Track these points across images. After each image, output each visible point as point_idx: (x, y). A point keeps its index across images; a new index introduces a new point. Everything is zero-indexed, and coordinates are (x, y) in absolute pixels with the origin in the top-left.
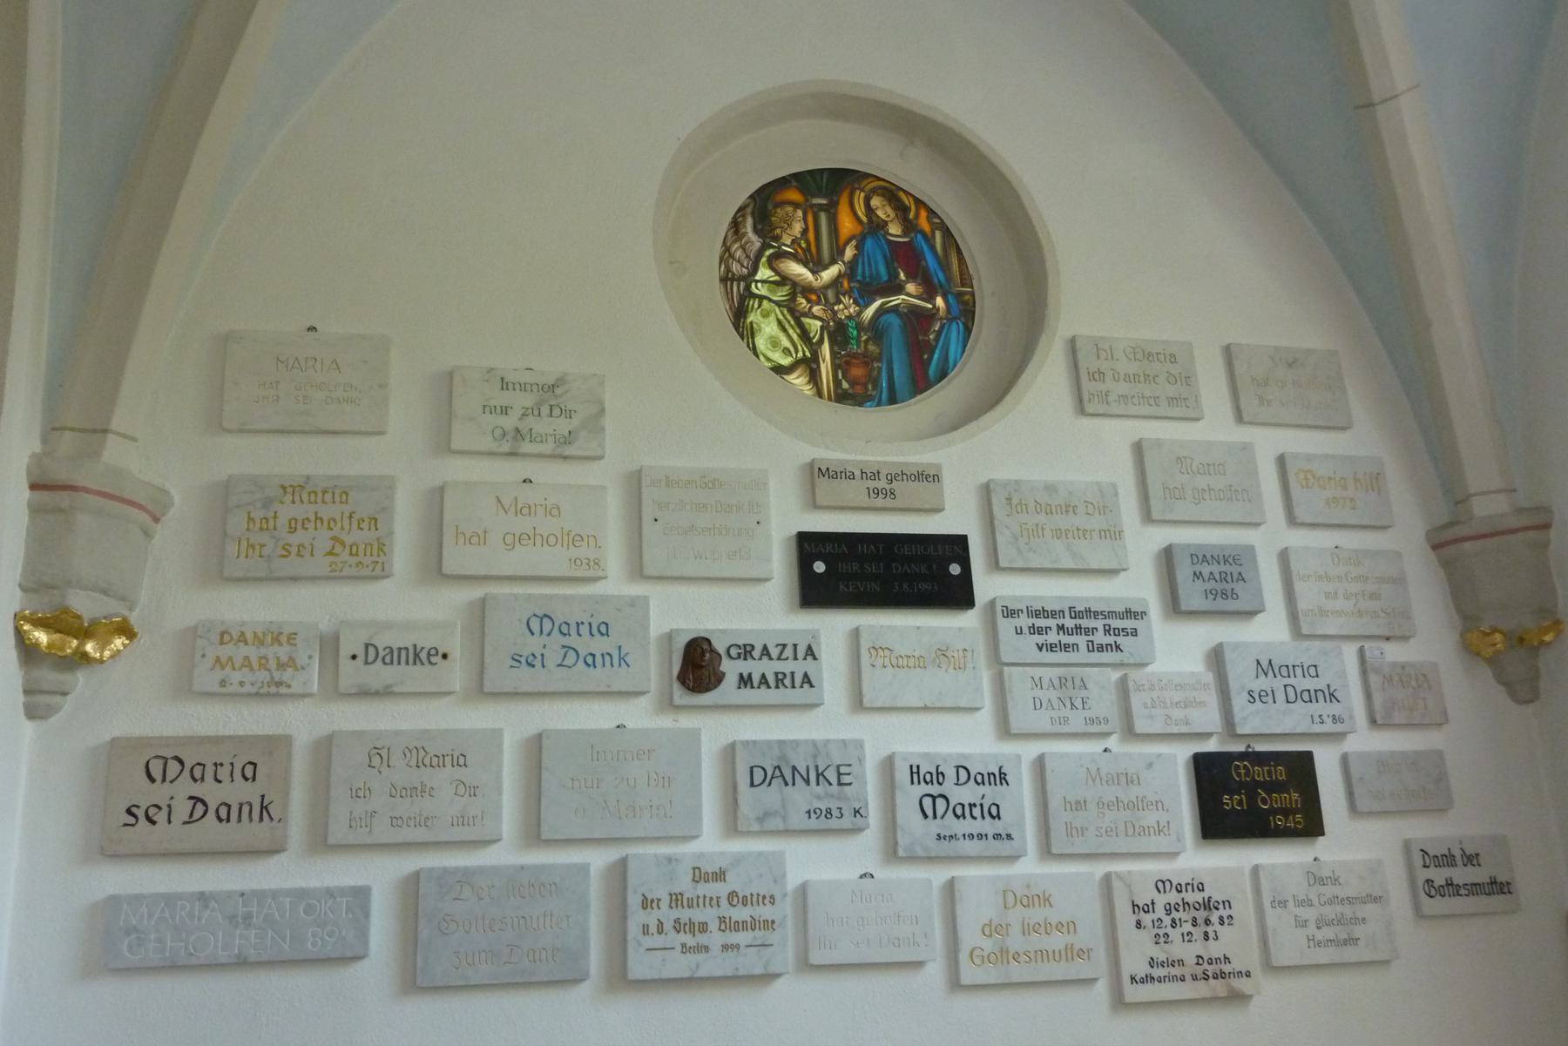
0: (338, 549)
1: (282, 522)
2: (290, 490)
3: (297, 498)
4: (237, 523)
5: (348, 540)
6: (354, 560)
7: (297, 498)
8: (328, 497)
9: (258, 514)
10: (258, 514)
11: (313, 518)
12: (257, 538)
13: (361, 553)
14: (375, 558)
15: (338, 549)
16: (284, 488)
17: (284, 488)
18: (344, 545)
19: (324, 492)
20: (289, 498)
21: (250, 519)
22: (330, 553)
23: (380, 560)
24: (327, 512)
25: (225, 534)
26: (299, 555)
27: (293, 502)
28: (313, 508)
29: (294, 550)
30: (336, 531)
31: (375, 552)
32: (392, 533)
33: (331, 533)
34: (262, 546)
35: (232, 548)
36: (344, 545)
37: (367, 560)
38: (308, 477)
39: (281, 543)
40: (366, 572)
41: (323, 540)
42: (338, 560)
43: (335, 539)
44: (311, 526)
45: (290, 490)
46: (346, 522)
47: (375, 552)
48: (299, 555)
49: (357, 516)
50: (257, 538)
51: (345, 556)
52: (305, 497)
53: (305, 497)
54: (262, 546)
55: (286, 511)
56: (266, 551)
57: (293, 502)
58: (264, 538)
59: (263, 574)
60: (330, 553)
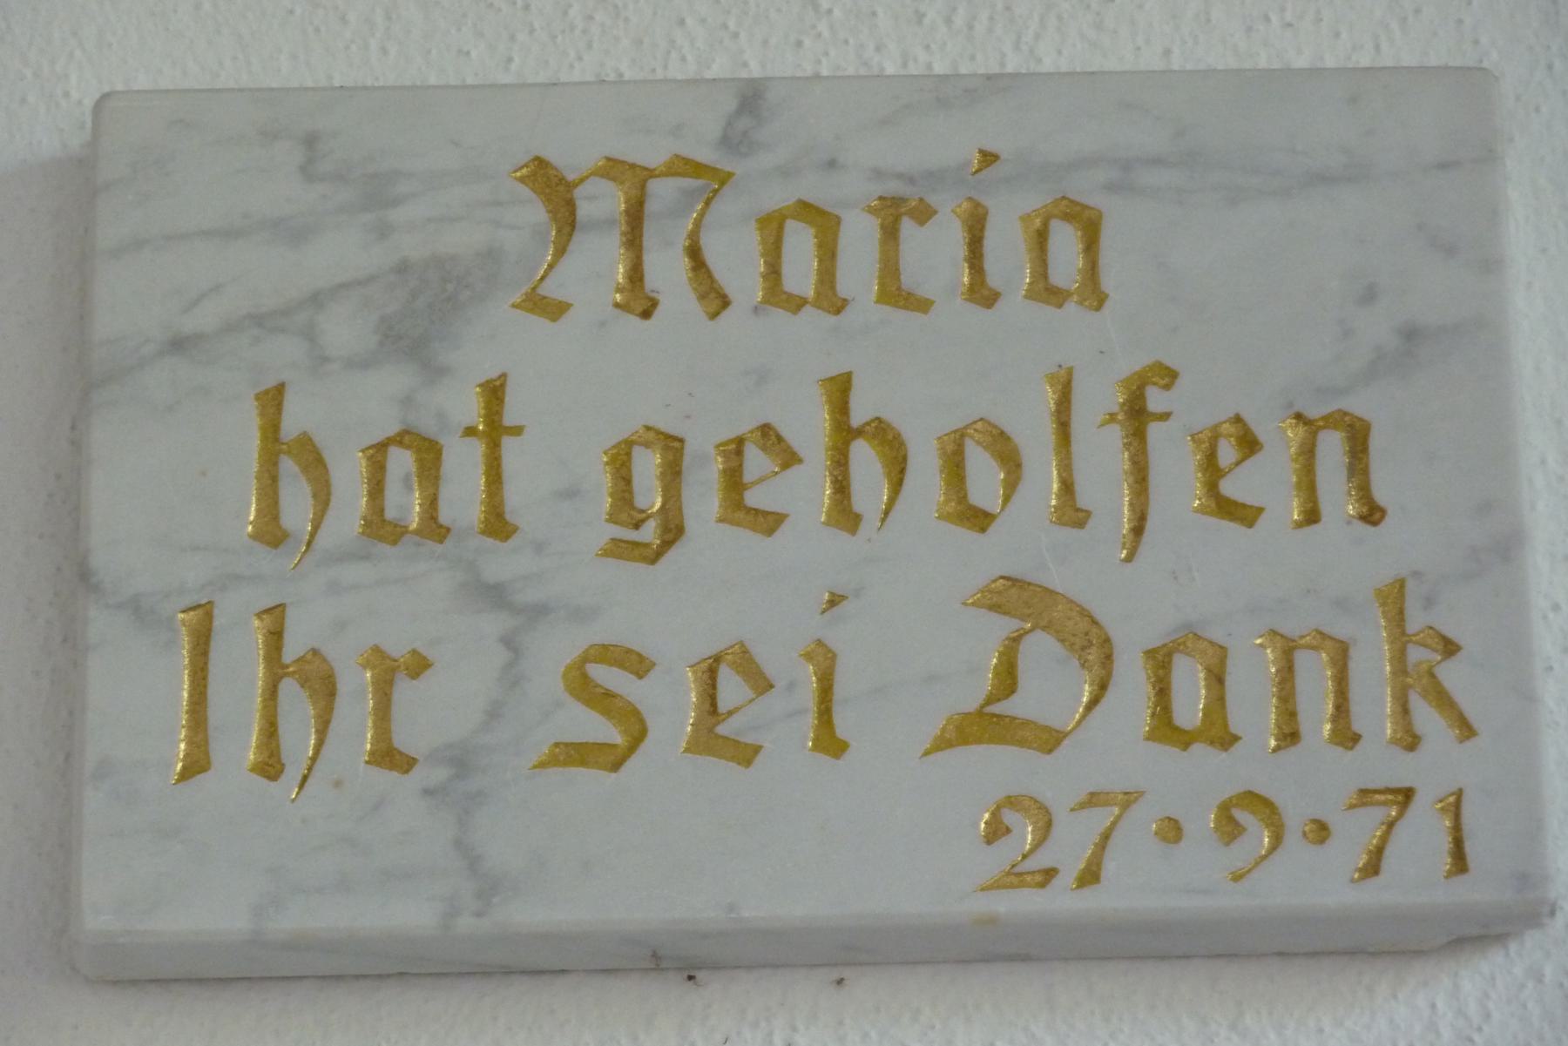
0: (1051, 685)
1: (555, 467)
2: (602, 202)
3: (666, 269)
4: (173, 490)
5: (1137, 611)
6: (1204, 777)
7: (666, 269)
8: (934, 253)
9: (348, 411)
10: (348, 411)
11: (809, 428)
12: (348, 609)
13: (1252, 709)
14: (1379, 762)
15: (1051, 685)
16: (552, 186)
17: (552, 186)
18: (1094, 647)
19: (896, 213)
20: (598, 261)
21: (286, 452)
22: (984, 725)
23: (1438, 764)
24: (923, 378)
25: (80, 576)
26: (713, 736)
27: (640, 301)
28: (809, 346)
29: (670, 704)
30: (1025, 539)
31: (1374, 709)
32: (1506, 548)
33: (989, 556)
34: (393, 671)
35: (135, 693)
36: (1094, 647)
37: (1315, 779)
38: (751, 98)
39: (554, 650)
40: (1314, 882)
41: (917, 611)
42: (1050, 777)
43: (1017, 598)
44: (802, 492)
45: (602, 202)
46: (1102, 454)
47: (1374, 709)
48: (713, 736)
49: (1185, 413)
50: (348, 609)
51: (1115, 742)
52: (736, 260)
53: (736, 260)
54: (393, 671)
55: (589, 377)
56: (426, 716)
57: (640, 301)
58: (404, 602)
59: (411, 914)
60: (984, 725)
